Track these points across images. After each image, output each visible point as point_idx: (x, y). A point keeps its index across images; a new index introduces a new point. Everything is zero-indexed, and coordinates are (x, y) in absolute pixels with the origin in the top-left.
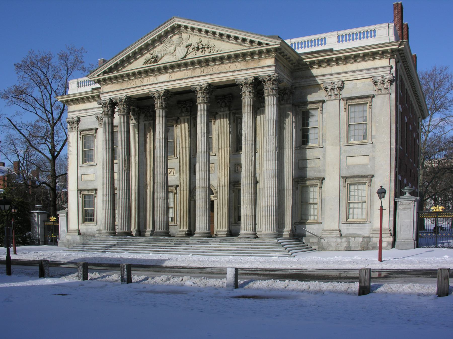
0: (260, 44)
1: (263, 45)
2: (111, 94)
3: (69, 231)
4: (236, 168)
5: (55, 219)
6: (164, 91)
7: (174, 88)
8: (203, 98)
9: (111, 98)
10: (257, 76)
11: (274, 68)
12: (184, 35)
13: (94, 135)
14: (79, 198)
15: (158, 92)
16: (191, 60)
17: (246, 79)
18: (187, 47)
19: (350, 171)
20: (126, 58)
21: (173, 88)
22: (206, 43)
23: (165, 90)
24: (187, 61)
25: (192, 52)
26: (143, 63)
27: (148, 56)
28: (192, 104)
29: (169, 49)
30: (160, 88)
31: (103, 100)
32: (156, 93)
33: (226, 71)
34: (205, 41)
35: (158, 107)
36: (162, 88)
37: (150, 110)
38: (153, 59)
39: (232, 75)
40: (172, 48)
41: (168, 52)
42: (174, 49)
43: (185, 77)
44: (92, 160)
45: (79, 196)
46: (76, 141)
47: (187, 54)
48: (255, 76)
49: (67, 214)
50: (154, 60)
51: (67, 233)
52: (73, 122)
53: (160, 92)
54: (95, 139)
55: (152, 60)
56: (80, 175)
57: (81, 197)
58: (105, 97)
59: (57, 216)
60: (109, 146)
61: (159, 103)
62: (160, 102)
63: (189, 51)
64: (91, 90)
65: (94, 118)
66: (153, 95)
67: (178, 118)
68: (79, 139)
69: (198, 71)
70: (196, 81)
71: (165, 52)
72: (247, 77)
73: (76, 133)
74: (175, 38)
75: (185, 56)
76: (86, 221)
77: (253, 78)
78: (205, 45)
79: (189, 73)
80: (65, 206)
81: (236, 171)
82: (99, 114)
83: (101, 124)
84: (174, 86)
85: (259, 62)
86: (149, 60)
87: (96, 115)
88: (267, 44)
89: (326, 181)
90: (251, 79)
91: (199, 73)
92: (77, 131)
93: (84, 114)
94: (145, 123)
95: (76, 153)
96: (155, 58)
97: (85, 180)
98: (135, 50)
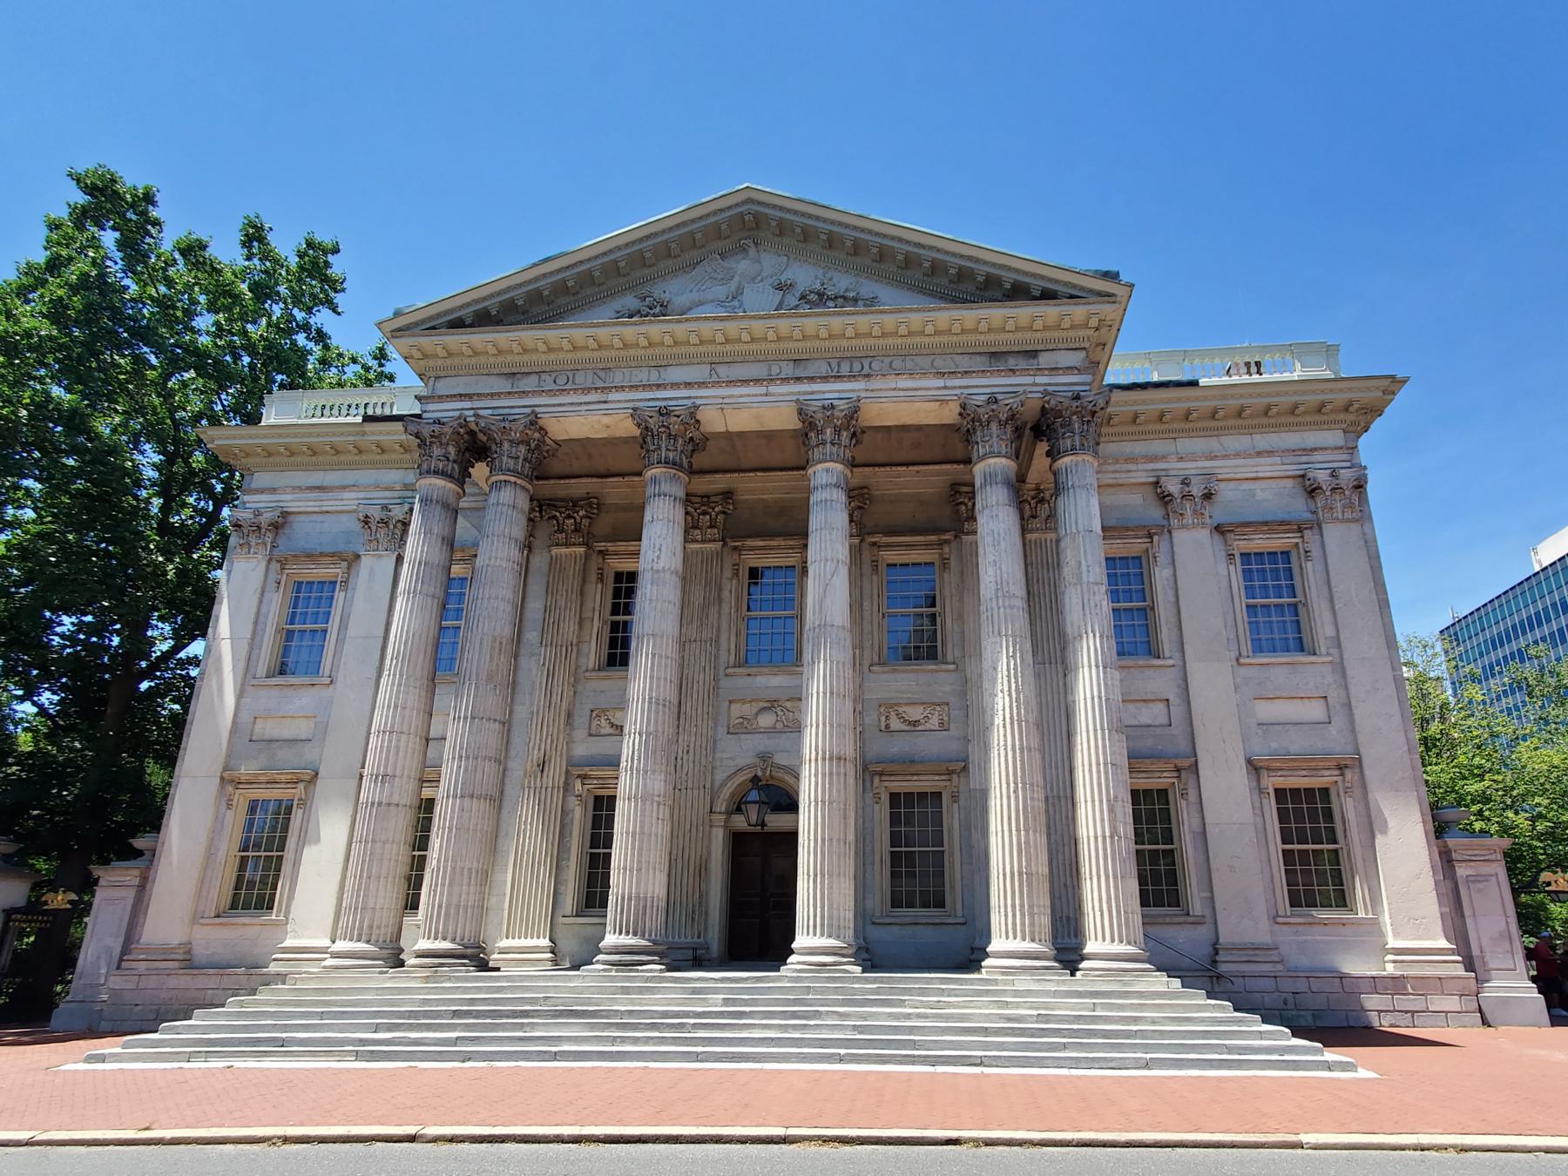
19: (1274, 745)
28: (731, 507)
37: (578, 512)
52: (259, 528)
54: (343, 594)
73: (264, 564)
92: (269, 561)
93: (311, 506)
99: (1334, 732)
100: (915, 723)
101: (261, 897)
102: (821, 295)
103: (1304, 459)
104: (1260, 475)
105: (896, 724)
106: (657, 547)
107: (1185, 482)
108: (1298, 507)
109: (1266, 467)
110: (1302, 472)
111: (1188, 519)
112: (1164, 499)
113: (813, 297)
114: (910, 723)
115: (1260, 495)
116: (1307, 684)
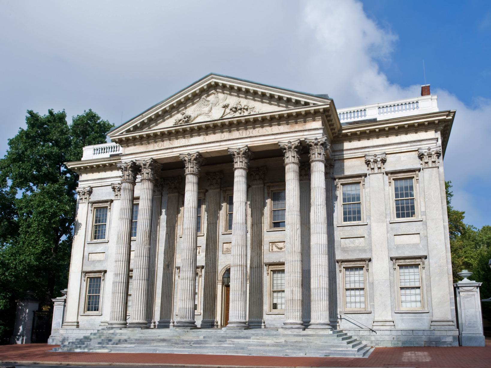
0: (307, 104)
1: (309, 105)
2: (133, 156)
3: (65, 324)
4: (271, 247)
5: (49, 309)
6: (197, 154)
8: (241, 163)
9: (134, 161)
10: (303, 139)
11: (321, 131)
12: (221, 96)
13: (109, 207)
14: (83, 281)
15: (189, 154)
16: (230, 120)
17: (290, 142)
18: (224, 107)
20: (155, 117)
21: (207, 152)
22: (246, 104)
23: (198, 152)
24: (224, 121)
25: (229, 113)
26: (174, 124)
27: (179, 116)
29: (204, 109)
30: (192, 151)
31: (124, 162)
32: (187, 156)
33: (267, 133)
35: (188, 172)
36: (193, 150)
37: (175, 181)
38: (185, 118)
39: (274, 138)
40: (206, 109)
41: (203, 112)
42: (210, 109)
43: (221, 140)
44: (103, 237)
45: (83, 279)
46: (86, 213)
47: (224, 115)
48: (301, 139)
49: (65, 301)
50: (186, 119)
51: (62, 325)
53: (192, 155)
55: (184, 119)
56: (86, 254)
57: (85, 280)
58: (126, 160)
59: (52, 305)
60: (128, 215)
61: (191, 167)
62: (192, 166)
63: (225, 113)
64: (109, 156)
65: (110, 189)
66: (184, 158)
67: (207, 191)
68: (89, 211)
69: (236, 134)
70: (234, 144)
71: (199, 113)
72: (291, 141)
74: (211, 98)
75: (222, 117)
76: (88, 310)
77: (298, 141)
78: (245, 106)
79: (226, 135)
80: (63, 292)
81: (271, 250)
82: (116, 184)
83: (117, 195)
84: (208, 149)
85: (305, 125)
86: (181, 120)
87: (113, 186)
88: (314, 104)
89: (373, 265)
90: (297, 143)
91: (237, 135)
92: (89, 203)
94: (169, 195)
95: (85, 228)
97: (92, 260)
98: (165, 108)
99: (421, 246)
100: (281, 249)
101: (95, 307)
102: (236, 108)
103: (419, 143)
104: (402, 151)
105: (275, 249)
106: (188, 200)
107: (375, 156)
109: (404, 147)
110: (417, 149)
111: (376, 170)
112: (368, 163)
113: (234, 109)
114: (279, 248)
115: (402, 159)
116: (413, 229)
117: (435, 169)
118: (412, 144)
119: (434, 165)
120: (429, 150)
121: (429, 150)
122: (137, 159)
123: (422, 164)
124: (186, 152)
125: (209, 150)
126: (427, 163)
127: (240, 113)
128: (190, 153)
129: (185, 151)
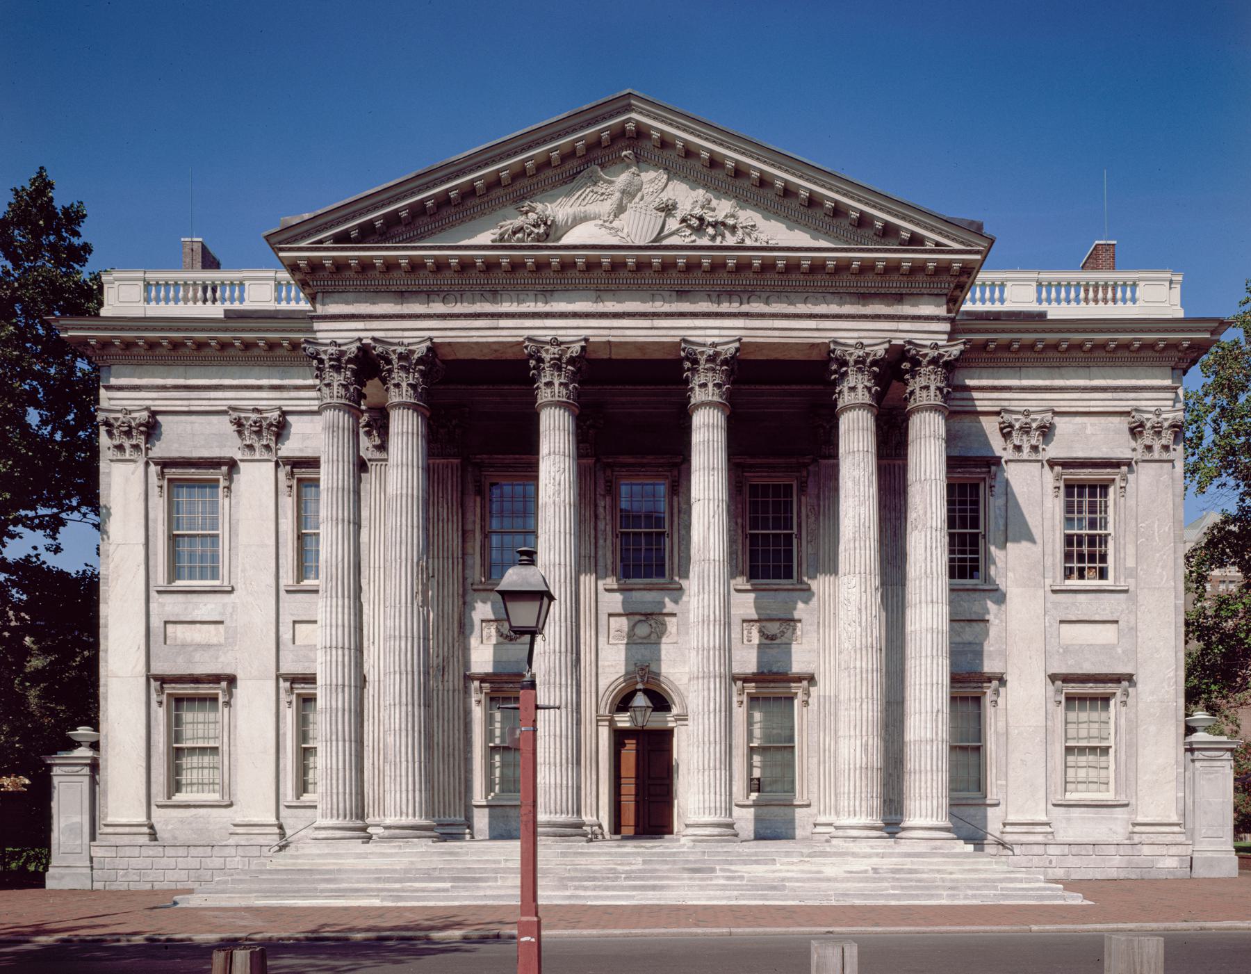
6: (583, 343)
7: (612, 339)
15: (555, 342)
18: (661, 210)
21: (609, 342)
25: (678, 230)
34: (723, 208)
38: (536, 225)
61: (561, 384)
96: (545, 224)
103: (1132, 395)
108: (1122, 447)
110: (1128, 409)
113: (695, 223)
117: (1166, 465)
118: (1116, 395)
119: (1165, 456)
120: (1158, 415)
121: (1158, 415)
122: (377, 334)
123: (1134, 450)
124: (547, 335)
125: (616, 336)
126: (1149, 448)
127: (713, 238)
128: (560, 339)
129: (544, 330)
